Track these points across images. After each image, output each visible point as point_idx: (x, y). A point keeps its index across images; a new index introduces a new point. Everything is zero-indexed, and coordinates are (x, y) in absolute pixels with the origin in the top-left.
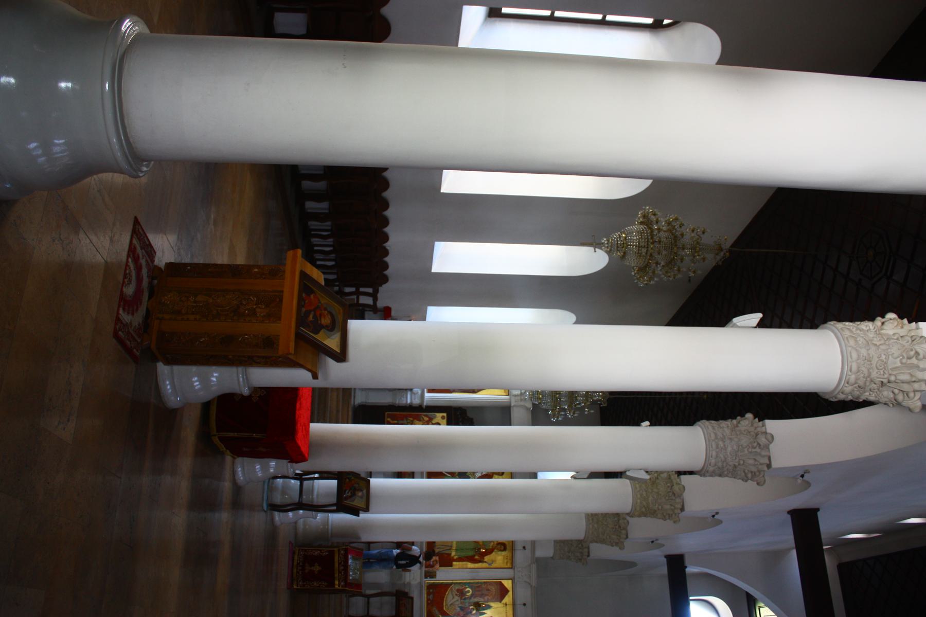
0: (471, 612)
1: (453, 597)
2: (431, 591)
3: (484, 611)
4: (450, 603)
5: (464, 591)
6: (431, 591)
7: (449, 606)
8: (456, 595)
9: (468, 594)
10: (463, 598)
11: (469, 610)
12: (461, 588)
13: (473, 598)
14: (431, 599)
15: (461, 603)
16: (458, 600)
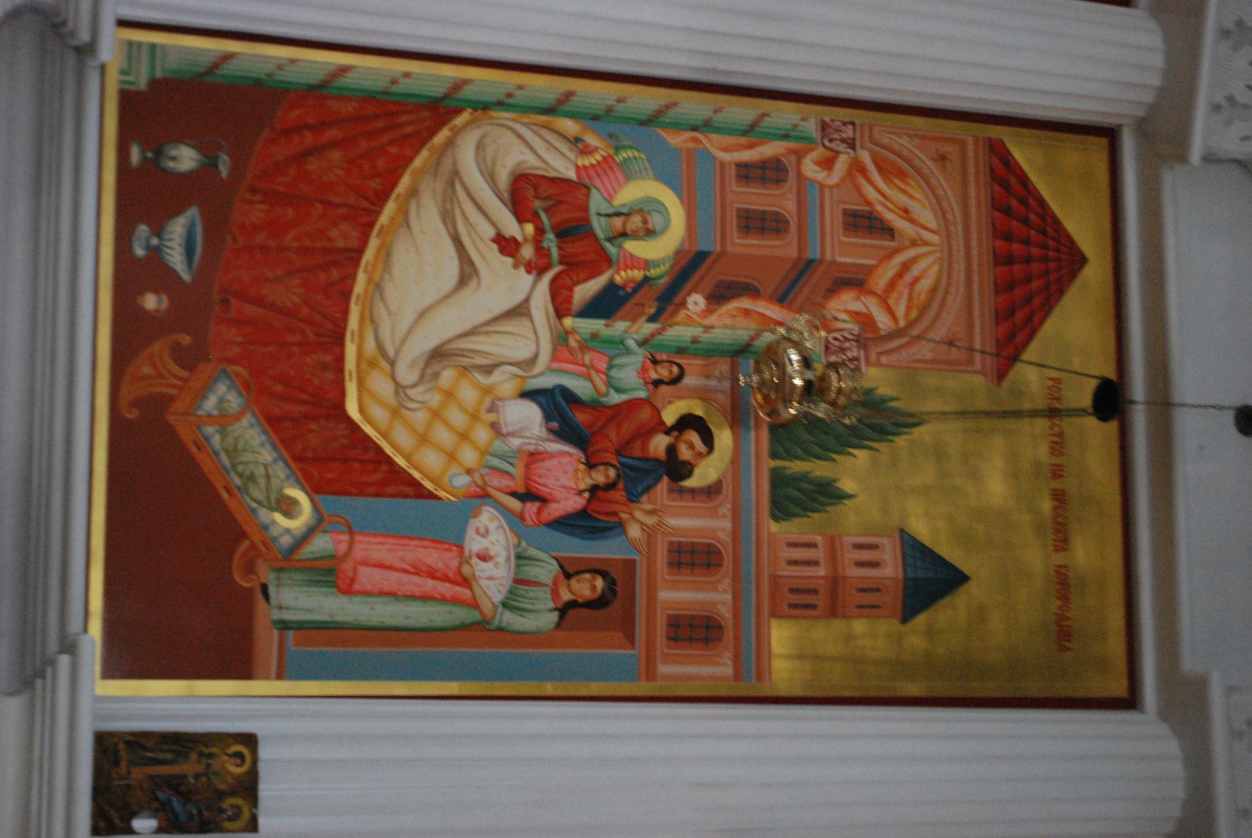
0: (677, 469)
1: (467, 273)
2: (185, 158)
3: (819, 469)
4: (421, 344)
5: (596, 202)
6: (185, 158)
7: (407, 375)
8: (507, 245)
9: (633, 247)
10: (586, 290)
11: (659, 443)
12: (563, 165)
13: (696, 302)
14: (176, 258)
15: (561, 340)
16: (520, 311)
